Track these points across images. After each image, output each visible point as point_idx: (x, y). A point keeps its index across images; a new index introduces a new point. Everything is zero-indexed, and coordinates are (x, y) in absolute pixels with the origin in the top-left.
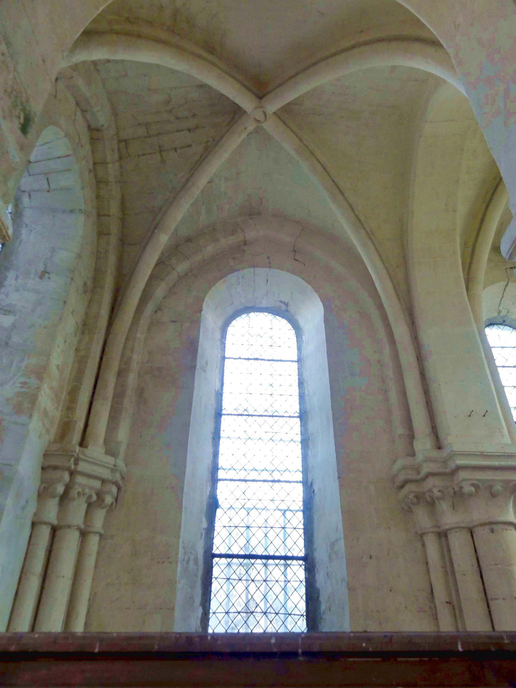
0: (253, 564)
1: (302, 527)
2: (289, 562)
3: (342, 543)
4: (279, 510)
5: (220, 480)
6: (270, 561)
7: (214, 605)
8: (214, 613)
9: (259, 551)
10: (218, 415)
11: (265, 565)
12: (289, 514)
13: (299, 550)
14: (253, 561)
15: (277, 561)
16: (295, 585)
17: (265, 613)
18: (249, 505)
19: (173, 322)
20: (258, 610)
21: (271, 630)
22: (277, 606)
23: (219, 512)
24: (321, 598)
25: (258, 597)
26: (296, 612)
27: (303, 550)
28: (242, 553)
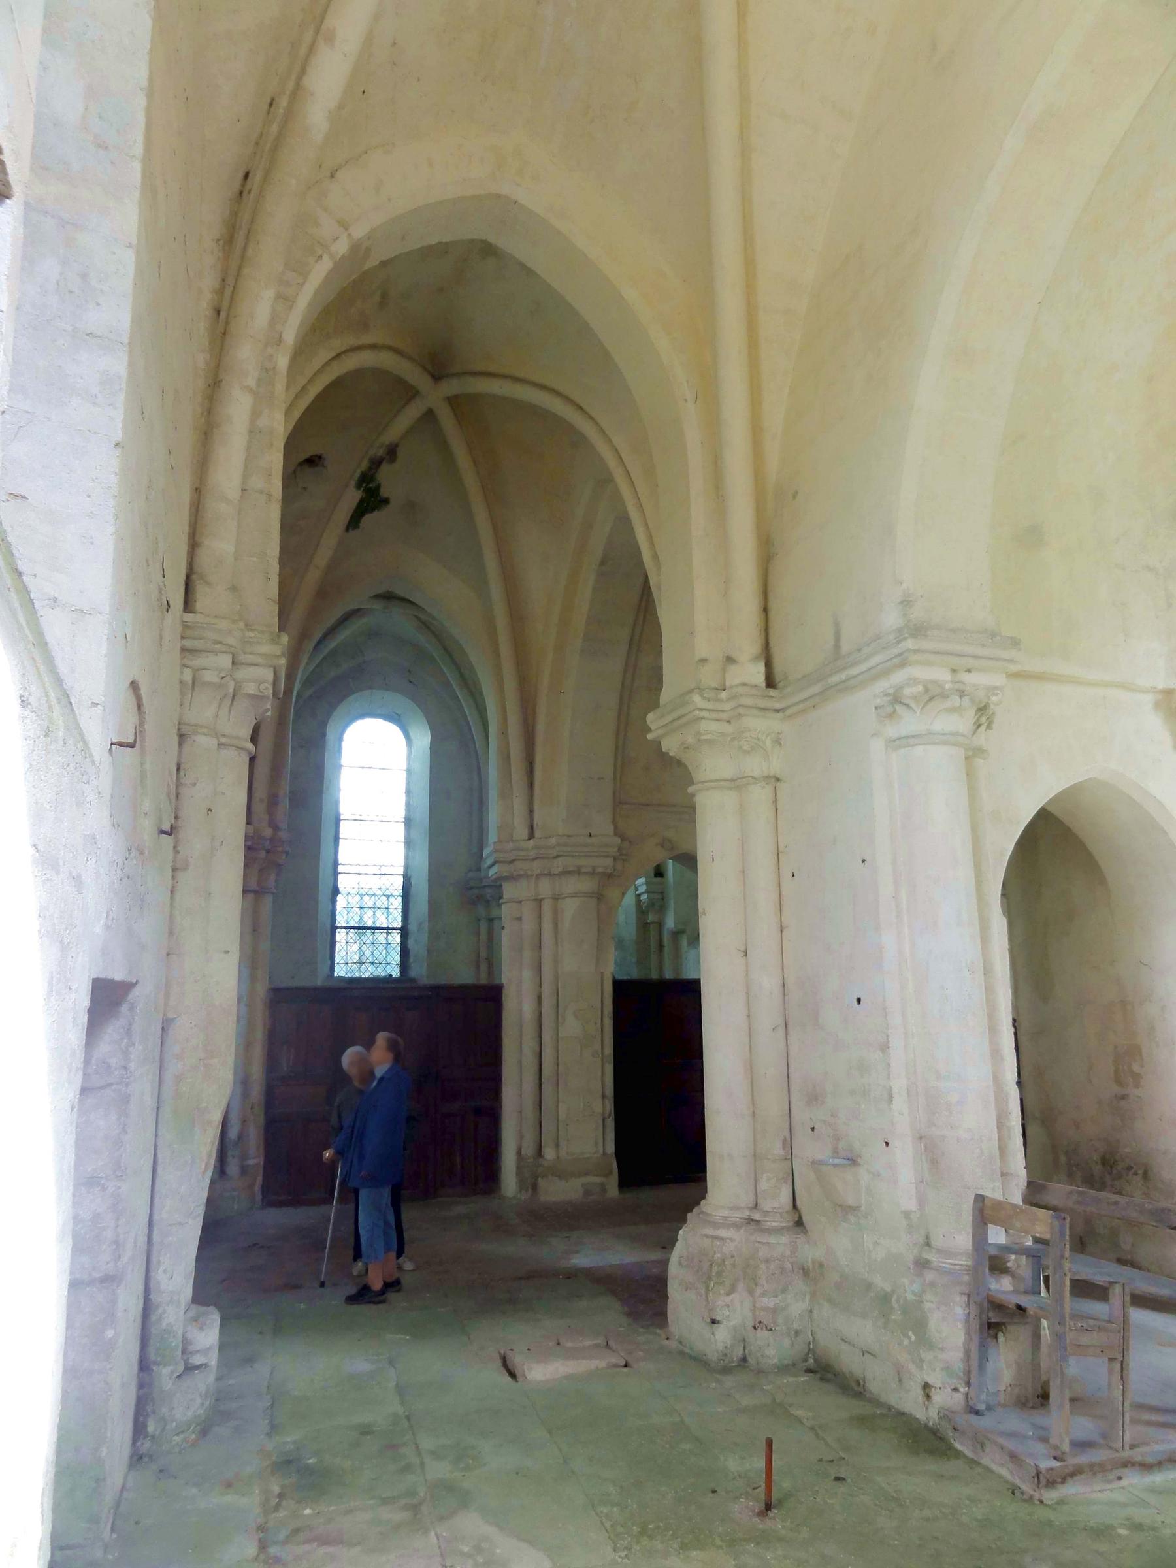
0: (365, 933)
1: (401, 907)
2: (390, 931)
3: (427, 924)
4: (385, 896)
5: (340, 873)
6: (377, 931)
7: (337, 959)
8: (338, 963)
9: (369, 924)
10: (337, 821)
11: (373, 933)
12: (392, 899)
13: (398, 924)
14: (364, 931)
15: (382, 931)
16: (394, 946)
17: (372, 963)
18: (362, 892)
19: (302, 747)
20: (368, 961)
21: (376, 974)
22: (381, 959)
23: (339, 898)
24: (411, 953)
25: (368, 953)
26: (393, 962)
27: (401, 923)
28: (357, 925)
